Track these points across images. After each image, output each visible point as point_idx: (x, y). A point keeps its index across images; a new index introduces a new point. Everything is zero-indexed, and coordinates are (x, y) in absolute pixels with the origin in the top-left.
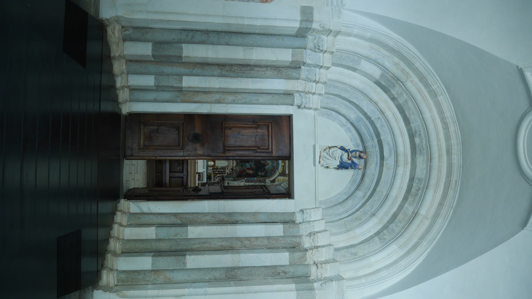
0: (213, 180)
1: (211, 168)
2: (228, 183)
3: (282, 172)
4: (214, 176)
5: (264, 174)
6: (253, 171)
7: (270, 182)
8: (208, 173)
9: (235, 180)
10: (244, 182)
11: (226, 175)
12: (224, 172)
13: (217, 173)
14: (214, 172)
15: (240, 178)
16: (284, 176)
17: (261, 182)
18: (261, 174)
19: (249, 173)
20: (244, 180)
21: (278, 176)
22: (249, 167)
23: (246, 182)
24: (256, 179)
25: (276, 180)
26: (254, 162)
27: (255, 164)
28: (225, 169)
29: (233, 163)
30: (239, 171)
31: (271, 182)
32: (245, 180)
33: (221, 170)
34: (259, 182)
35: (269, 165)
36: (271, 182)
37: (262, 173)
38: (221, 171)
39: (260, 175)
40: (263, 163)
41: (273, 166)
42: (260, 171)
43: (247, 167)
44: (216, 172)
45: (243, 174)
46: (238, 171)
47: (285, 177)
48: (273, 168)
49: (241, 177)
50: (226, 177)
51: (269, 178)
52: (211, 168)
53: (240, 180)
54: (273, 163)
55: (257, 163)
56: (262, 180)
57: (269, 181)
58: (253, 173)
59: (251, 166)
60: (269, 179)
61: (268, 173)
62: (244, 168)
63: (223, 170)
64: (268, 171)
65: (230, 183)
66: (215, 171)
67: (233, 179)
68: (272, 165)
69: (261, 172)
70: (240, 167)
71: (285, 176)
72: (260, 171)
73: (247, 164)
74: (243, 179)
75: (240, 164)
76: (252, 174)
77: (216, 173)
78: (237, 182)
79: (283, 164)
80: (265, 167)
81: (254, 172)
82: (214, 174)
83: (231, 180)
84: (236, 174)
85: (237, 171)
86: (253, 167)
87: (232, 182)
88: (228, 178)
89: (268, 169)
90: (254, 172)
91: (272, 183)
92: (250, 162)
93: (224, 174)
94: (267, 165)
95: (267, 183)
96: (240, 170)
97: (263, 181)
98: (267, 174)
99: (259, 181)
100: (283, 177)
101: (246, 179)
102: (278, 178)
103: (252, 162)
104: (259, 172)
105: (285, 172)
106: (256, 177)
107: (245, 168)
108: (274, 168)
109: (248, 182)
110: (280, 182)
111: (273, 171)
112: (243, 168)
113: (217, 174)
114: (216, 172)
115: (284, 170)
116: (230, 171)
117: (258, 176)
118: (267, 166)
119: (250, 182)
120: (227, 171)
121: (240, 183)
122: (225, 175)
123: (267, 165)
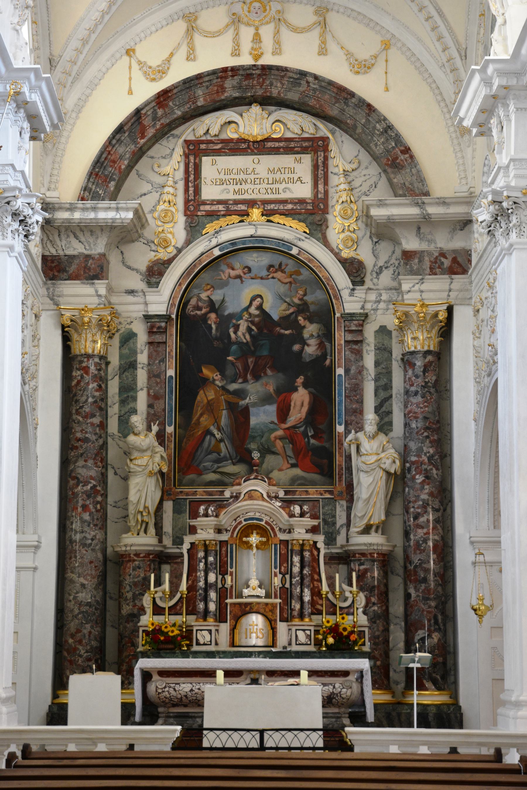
0: (347, 621)
1: (282, 627)
2: (367, 530)
3: (300, 221)
4: (332, 610)
5: (311, 322)
6: (296, 390)
7: (360, 292)
8: (312, 648)
9: (350, 487)
10: (360, 435)
11: (320, 539)
12: (307, 554)
13: (312, 595)
14: (308, 610)
15: (339, 460)
16: (325, 211)
17: (361, 342)
18: (313, 342)
19: (305, 409)
20: (351, 437)
21: (326, 243)
22: (272, 409)
23: (360, 428)
24: (340, 371)
25: (346, 254)
26: (245, 381)
27: (257, 377)
28: (287, 541)
29: (250, 496)
30: (293, 466)
31: (362, 283)
32: (347, 432)
33: (296, 569)
34: (359, 354)
35: (260, 296)
36: (362, 283)
37: (306, 335)
38: (302, 567)
39: (321, 345)
40: (249, 330)
41: (264, 273)
42: (296, 347)
43: (276, 421)
44: (307, 598)
45: (312, 441)
46: (297, 471)
47: (331, 203)
48: (279, 275)
49: (330, 456)
50: (330, 540)
51: (339, 297)
52: (282, 627)
53: (349, 458)
54: (250, 270)
55: (251, 361)
56: (349, 337)
57: (351, 295)
58: (305, 385)
59: (266, 400)
60: (345, 294)
61: (309, 298)
62: (281, 438)
63: (296, 559)
64: (296, 301)
65: (365, 521)
66: (298, 607)
67: (344, 503)
68: (262, 278)
69: (304, 343)
70: (270, 459)
71: (326, 205)
72: (296, 347)
73: (253, 421)
74: (341, 444)
75: (256, 455)
76: (310, 393)
77: (313, 603)
78: (362, 475)
79: (256, 213)
80: (275, 317)
81: (300, 380)
82: (320, 613)
83: (349, 509)
84: (313, 483)
85: (293, 481)
86: (271, 389)
87: (359, 509)
88: (339, 532)
89: (281, 298)
90: (300, 380)
91: (367, 279)
92: (243, 403)
93: (318, 550)
94: (260, 307)
95: (363, 307)
96: (293, 461)
97: (354, 328)
98: (312, 308)
99: (352, 351)
100: (330, 217)
101: (340, 429)
102: (335, 247)
103: (240, 394)
104: (302, 349)
105: (302, 201)
106: (331, 370)
107: (280, 433)
108: (280, 268)
109: (360, 412)
110: (360, 234)
111: (298, 273)
112: (279, 444)
113: (316, 593)
114: (307, 598)
115: (290, 206)
116: (302, 515)
117: (324, 356)
118: (266, 307)
119: (361, 402)
120: (297, 530)
121: (363, 458)
122: (321, 545)
123: (260, 307)
